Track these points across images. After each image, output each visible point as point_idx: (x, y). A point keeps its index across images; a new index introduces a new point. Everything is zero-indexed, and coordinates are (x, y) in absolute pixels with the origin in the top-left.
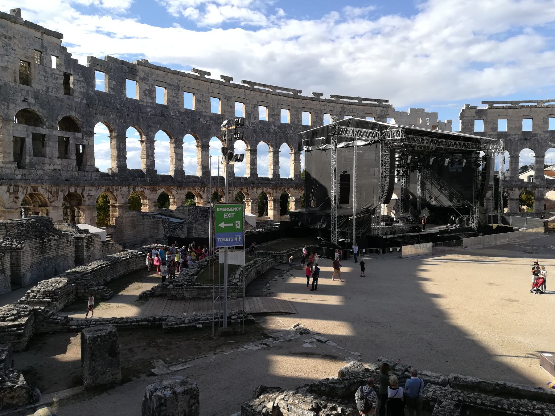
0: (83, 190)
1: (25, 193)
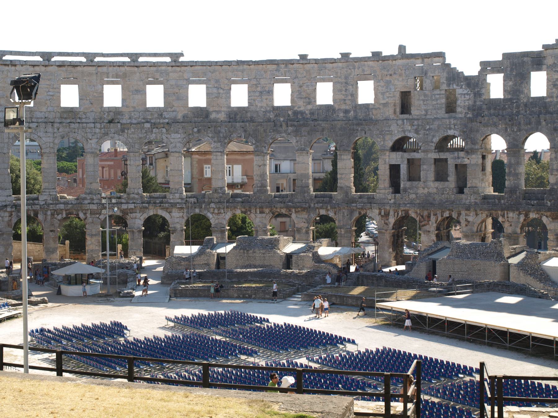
0: (459, 214)
1: (396, 216)
